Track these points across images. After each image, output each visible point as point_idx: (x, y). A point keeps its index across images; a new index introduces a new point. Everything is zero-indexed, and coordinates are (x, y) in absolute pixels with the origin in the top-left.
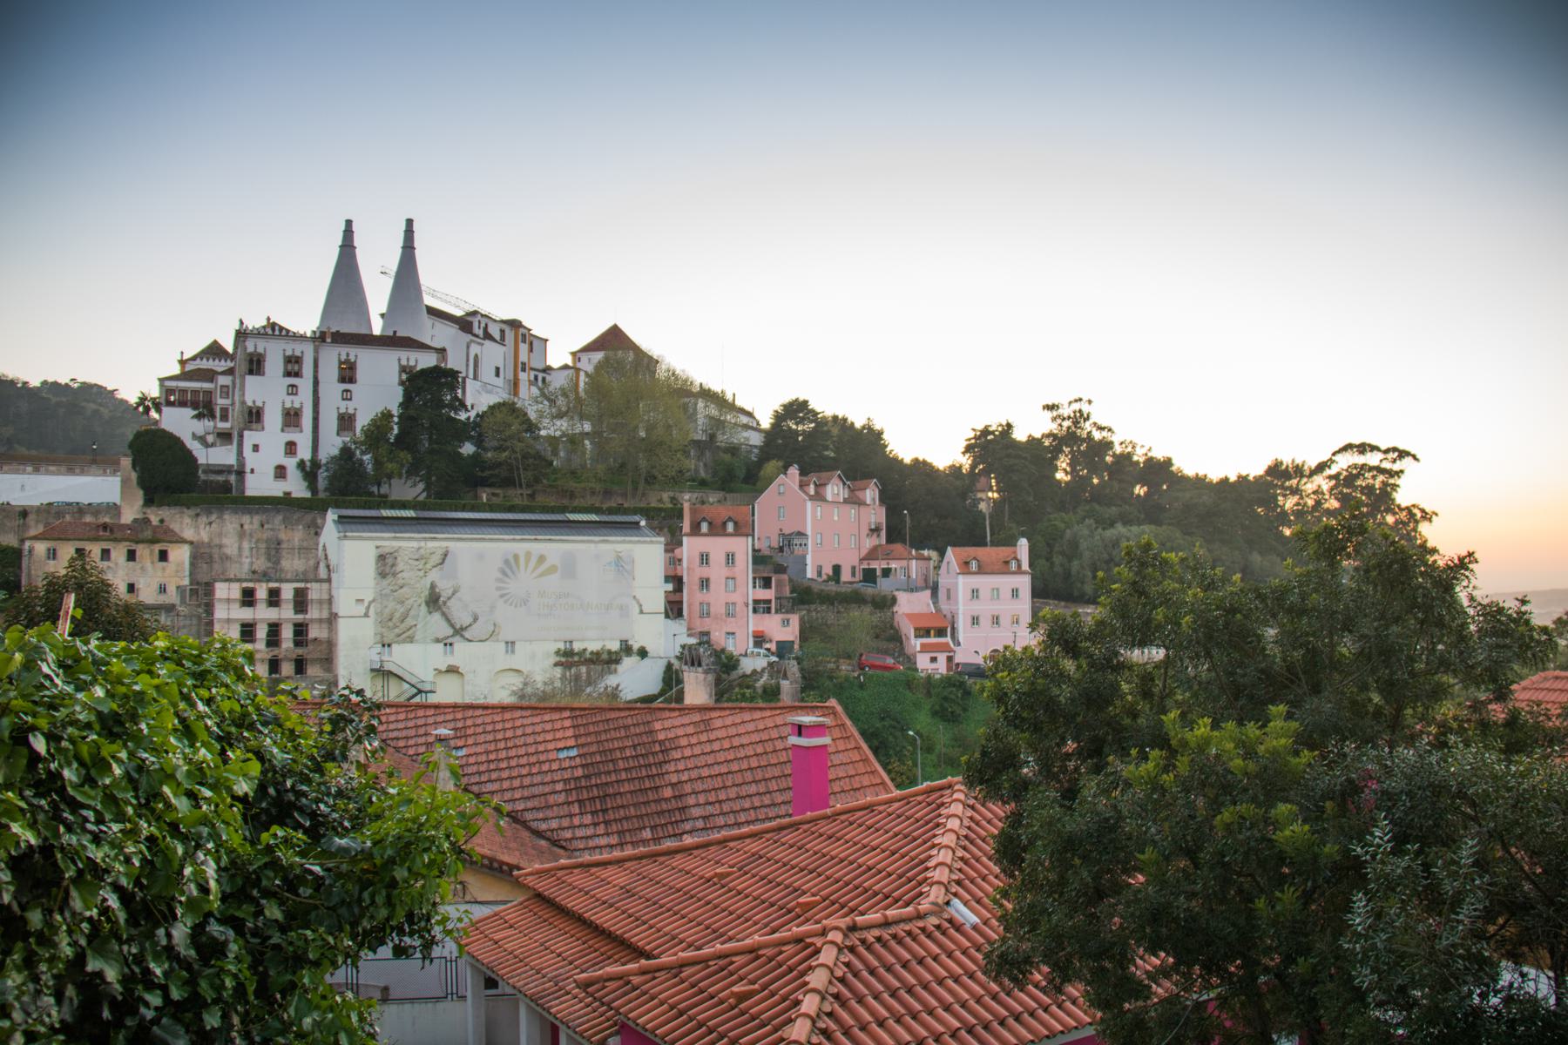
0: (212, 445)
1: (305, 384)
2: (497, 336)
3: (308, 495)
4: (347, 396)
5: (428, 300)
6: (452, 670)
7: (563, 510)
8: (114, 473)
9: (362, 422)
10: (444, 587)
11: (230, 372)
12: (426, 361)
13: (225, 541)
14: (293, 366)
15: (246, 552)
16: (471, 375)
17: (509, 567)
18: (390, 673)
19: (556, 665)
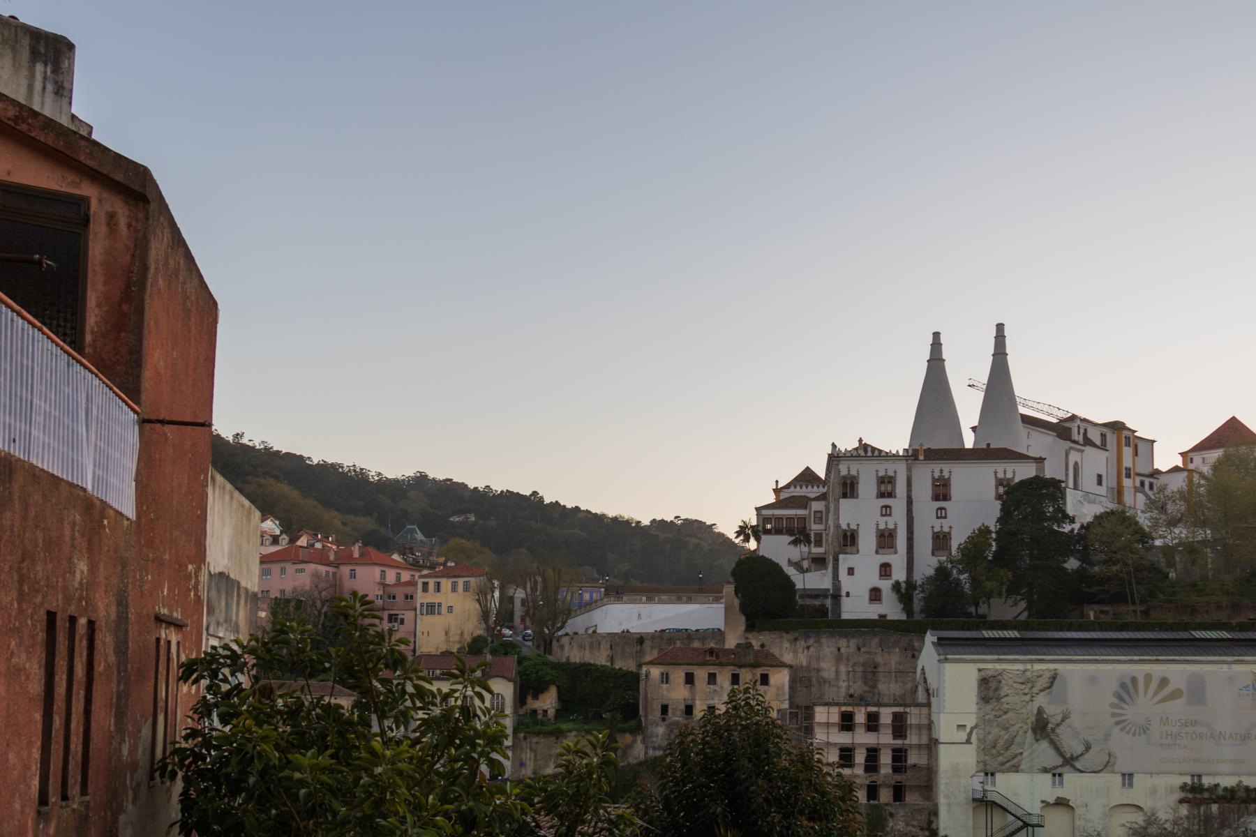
0: (808, 570)
1: (898, 505)
2: (1098, 442)
3: (904, 617)
4: (941, 514)
5: (1022, 410)
6: (1061, 803)
7: (1186, 627)
8: (717, 600)
9: (957, 541)
10: (1053, 711)
11: (823, 497)
12: (1024, 472)
13: (823, 665)
14: (886, 487)
15: (843, 677)
16: (1071, 484)
17: (1126, 691)
18: (994, 803)
19: (1181, 801)
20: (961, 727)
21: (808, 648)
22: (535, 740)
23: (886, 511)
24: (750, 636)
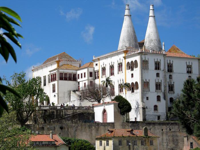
4: (170, 77)
14: (157, 66)
15: (165, 141)
21: (150, 129)
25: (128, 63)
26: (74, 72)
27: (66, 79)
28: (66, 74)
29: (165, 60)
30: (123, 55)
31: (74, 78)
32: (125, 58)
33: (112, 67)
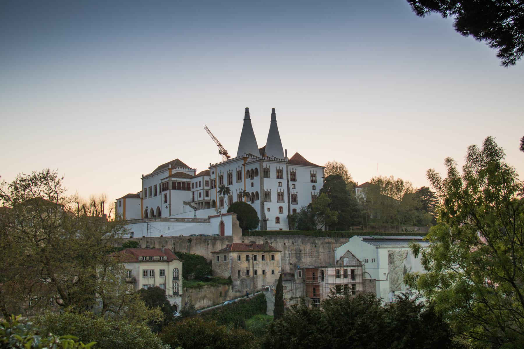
1: (284, 181)
3: (288, 230)
15: (287, 256)
20: (385, 274)
21: (271, 243)
22: (191, 291)
23: (280, 185)
24: (245, 238)
25: (248, 171)
26: (188, 180)
27: (179, 188)
28: (179, 183)
29: (287, 168)
30: (242, 162)
31: (186, 187)
32: (244, 165)
33: (230, 176)
